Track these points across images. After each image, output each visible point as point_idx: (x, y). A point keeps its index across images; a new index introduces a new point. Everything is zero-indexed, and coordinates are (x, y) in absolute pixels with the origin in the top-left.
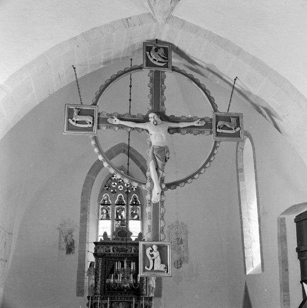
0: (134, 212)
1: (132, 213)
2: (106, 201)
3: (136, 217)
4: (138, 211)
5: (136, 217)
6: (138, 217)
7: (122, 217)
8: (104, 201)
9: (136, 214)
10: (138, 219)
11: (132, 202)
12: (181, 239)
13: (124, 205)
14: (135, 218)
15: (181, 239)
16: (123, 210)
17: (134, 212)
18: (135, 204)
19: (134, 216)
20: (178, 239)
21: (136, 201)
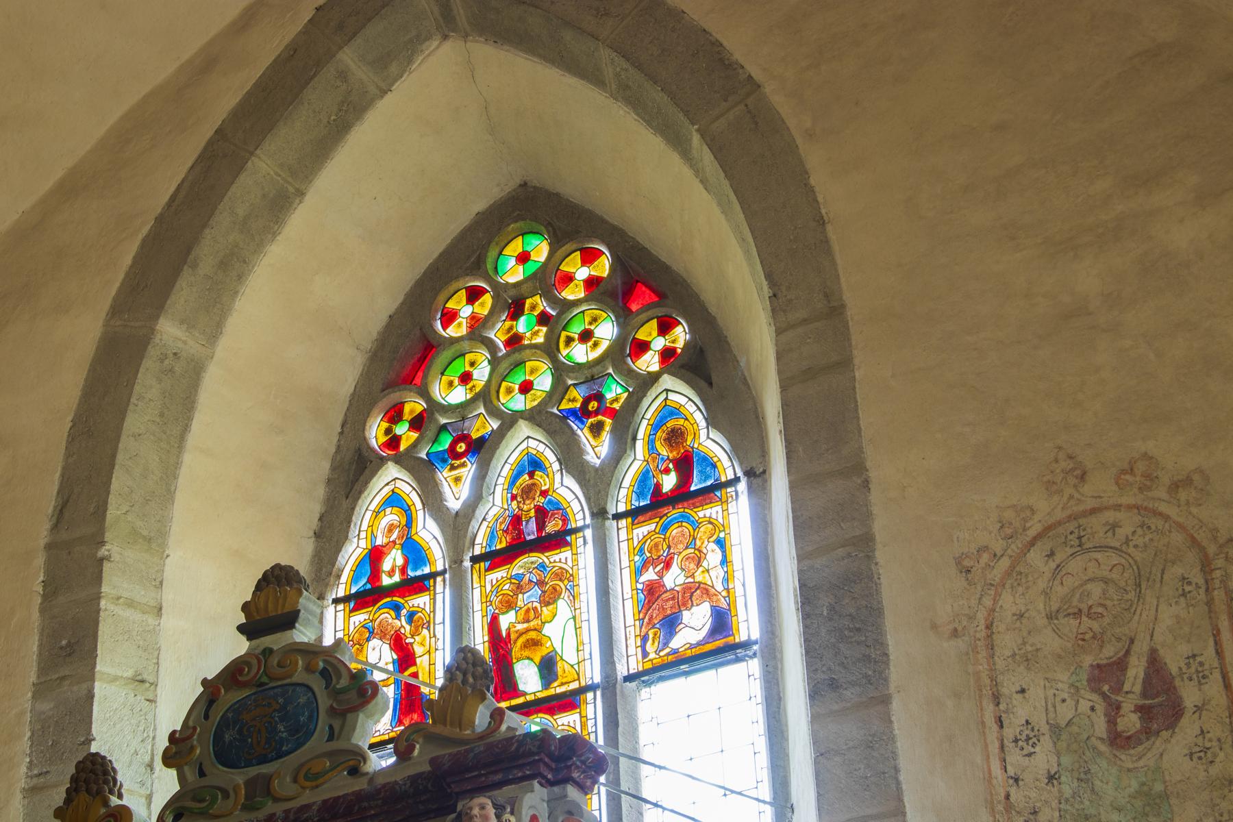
0: (674, 578)
1: (653, 591)
2: (394, 558)
3: (695, 624)
4: (713, 556)
5: (695, 624)
6: (721, 622)
7: (548, 667)
8: (376, 555)
9: (691, 592)
10: (721, 646)
11: (644, 477)
12: (1154, 662)
13: (557, 541)
14: (685, 638)
15: (1154, 662)
16: (549, 599)
17: (674, 578)
18: (682, 495)
19: (671, 624)
20: (1107, 676)
21: (684, 464)
